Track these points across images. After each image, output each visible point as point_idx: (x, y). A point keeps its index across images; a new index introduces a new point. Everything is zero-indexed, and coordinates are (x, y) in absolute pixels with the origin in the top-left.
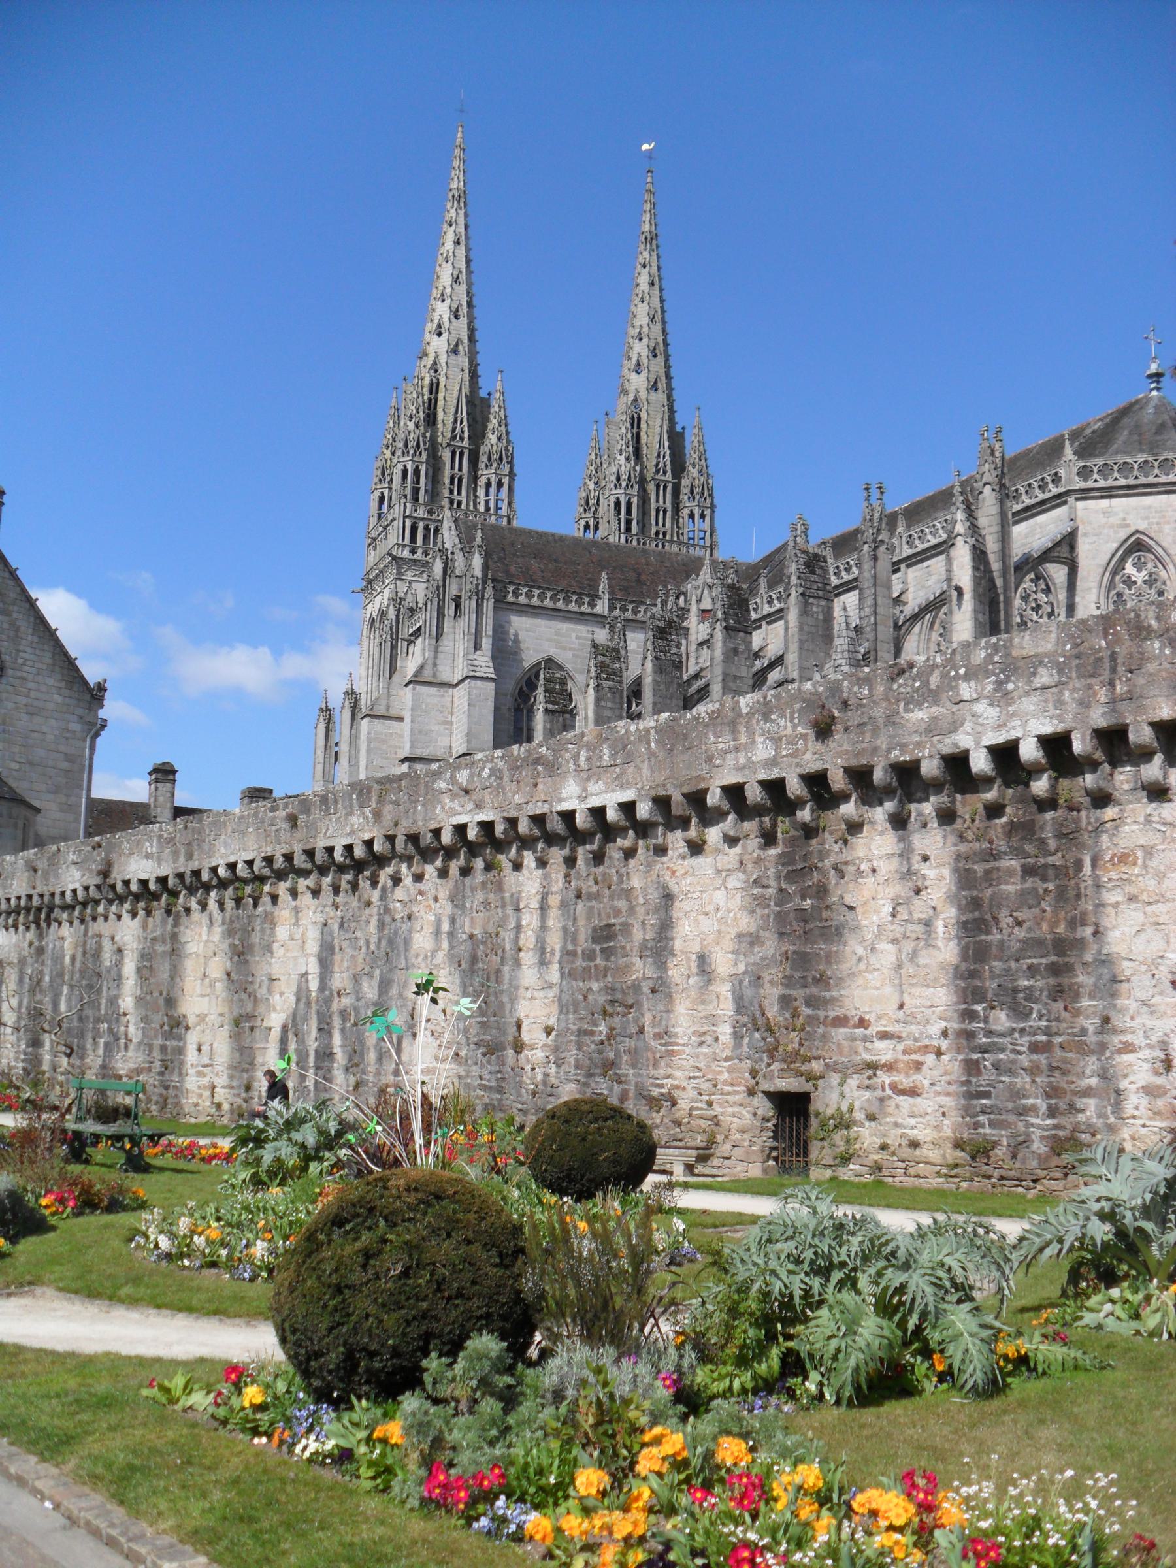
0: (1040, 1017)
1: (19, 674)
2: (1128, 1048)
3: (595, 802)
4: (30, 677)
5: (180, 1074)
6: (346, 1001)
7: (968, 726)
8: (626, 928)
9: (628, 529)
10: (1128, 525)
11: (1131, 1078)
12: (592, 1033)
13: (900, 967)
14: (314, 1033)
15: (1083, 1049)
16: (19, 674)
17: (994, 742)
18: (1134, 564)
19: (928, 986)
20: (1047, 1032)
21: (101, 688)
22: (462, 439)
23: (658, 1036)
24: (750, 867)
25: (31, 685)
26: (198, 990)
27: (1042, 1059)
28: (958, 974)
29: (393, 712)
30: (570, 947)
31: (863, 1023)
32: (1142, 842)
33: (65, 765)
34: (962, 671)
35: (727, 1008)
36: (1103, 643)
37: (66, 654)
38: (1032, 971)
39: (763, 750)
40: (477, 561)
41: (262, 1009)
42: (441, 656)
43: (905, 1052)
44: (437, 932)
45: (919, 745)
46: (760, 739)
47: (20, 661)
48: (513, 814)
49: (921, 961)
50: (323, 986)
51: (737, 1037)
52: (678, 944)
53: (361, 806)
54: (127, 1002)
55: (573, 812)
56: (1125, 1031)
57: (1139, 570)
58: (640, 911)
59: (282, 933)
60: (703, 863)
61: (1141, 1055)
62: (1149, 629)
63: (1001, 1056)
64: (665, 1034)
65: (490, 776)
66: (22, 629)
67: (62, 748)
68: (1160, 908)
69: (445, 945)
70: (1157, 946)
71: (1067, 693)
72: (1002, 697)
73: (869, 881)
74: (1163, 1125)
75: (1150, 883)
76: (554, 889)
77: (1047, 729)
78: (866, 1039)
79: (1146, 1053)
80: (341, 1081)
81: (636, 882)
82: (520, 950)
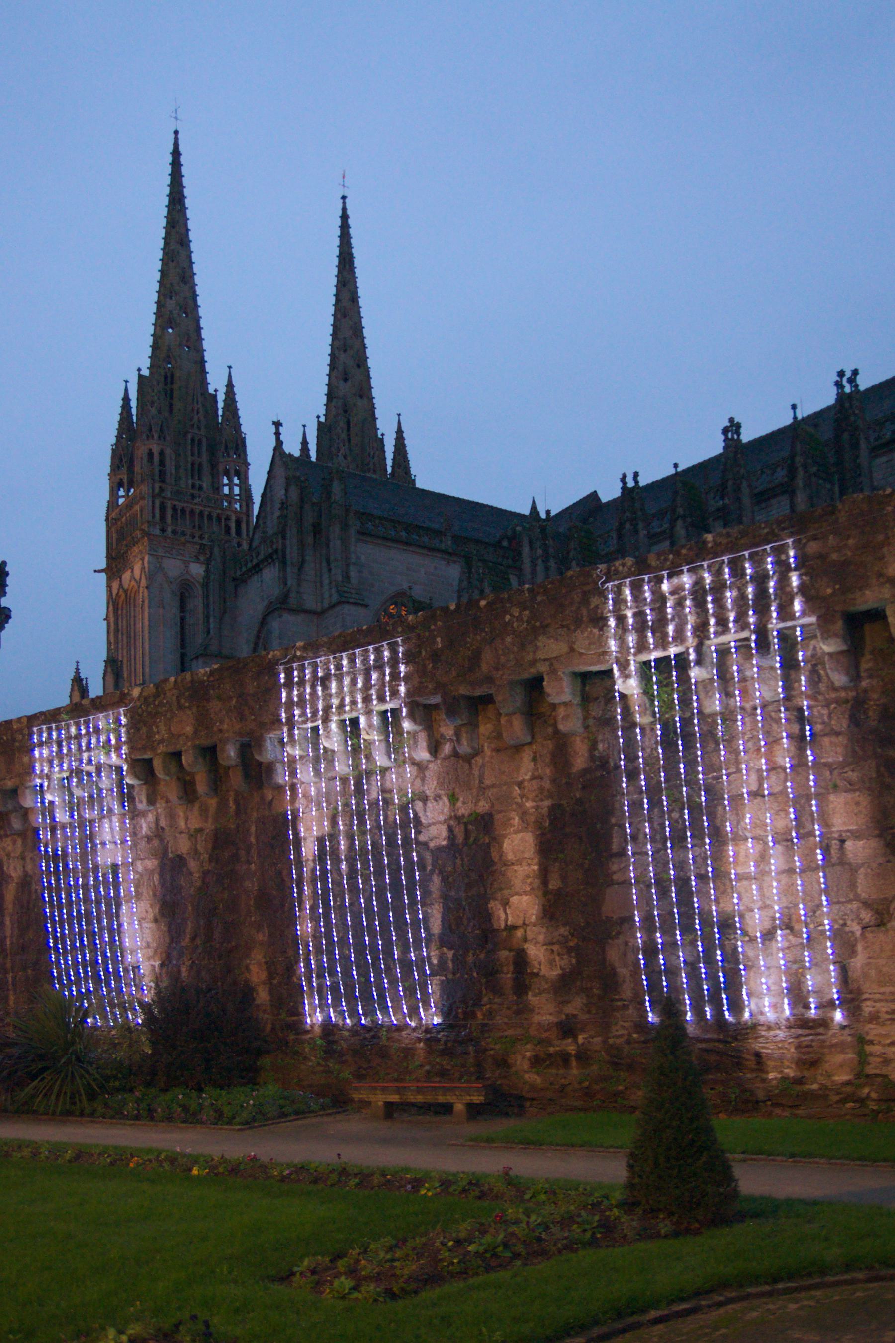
22: (199, 428)
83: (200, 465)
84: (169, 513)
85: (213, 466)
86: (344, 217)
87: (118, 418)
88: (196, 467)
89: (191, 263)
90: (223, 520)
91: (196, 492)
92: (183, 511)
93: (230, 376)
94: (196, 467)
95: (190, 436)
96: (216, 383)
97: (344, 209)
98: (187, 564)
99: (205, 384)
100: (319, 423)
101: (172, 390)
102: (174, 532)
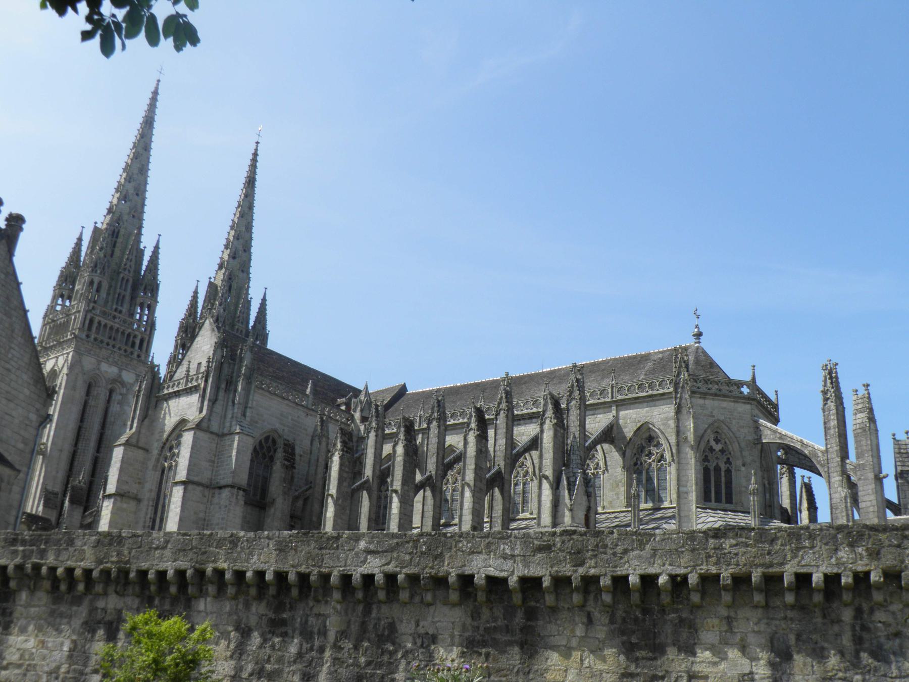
4: (13, 370)
10: (713, 416)
16: (8, 366)
18: (714, 440)
29: (140, 445)
33: (21, 446)
57: (717, 443)
83: (124, 297)
84: (95, 325)
85: (133, 298)
86: (255, 154)
87: (71, 250)
88: (121, 297)
89: (149, 162)
90: (132, 337)
92: (105, 326)
93: (158, 241)
94: (121, 297)
95: (121, 275)
96: (147, 243)
97: (256, 150)
98: (99, 362)
99: (138, 241)
100: (210, 283)
101: (115, 242)
102: (95, 339)
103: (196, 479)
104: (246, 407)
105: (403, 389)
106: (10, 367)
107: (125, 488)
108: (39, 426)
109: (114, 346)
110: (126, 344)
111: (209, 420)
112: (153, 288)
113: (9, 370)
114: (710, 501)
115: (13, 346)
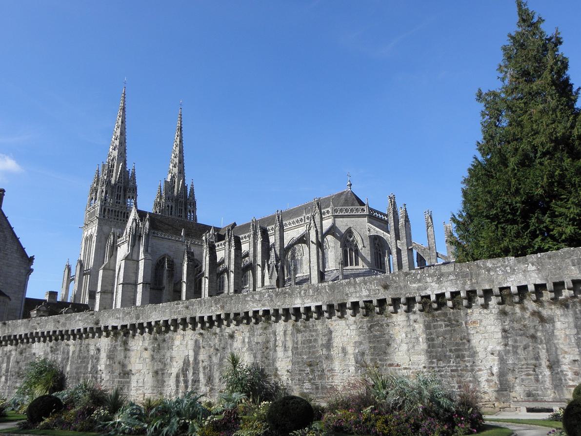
0: (453, 363)
1: (5, 252)
2: (480, 370)
3: (307, 305)
4: (9, 254)
5: (128, 390)
6: (206, 363)
7: (429, 289)
8: (316, 340)
9: (171, 214)
11: (482, 378)
12: (305, 371)
13: (409, 350)
14: (191, 374)
15: (467, 371)
16: (5, 252)
17: (437, 293)
19: (418, 355)
20: (456, 366)
21: (32, 259)
23: (329, 371)
24: (358, 324)
25: (9, 256)
26: (137, 361)
27: (455, 373)
28: (427, 352)
29: (111, 268)
30: (295, 346)
31: (398, 365)
32: (479, 318)
33: (18, 284)
34: (427, 275)
35: (352, 362)
36: (468, 270)
37: (22, 247)
38: (451, 351)
39: (365, 293)
40: (147, 224)
41: (168, 367)
42: (134, 252)
43: (412, 373)
44: (244, 342)
45: (415, 293)
46: (363, 290)
47: (6, 248)
48: (277, 308)
49: (416, 348)
50: (196, 359)
51: (357, 371)
52: (335, 344)
53: (216, 304)
54: (101, 366)
55: (300, 308)
56: (479, 366)
58: (320, 336)
59: (177, 343)
60: (342, 322)
61: (484, 372)
62: (481, 267)
63: (442, 373)
64: (332, 370)
65: (268, 297)
66: (8, 238)
67: (18, 279)
68: (486, 335)
69: (247, 346)
70: (486, 343)
71: (458, 281)
72: (439, 281)
73: (397, 328)
74: (493, 389)
75: (482, 328)
76: (289, 329)
77: (454, 290)
78: (399, 369)
79: (485, 372)
80: (203, 389)
81: (319, 327)
82: (277, 346)
83: (120, 195)
85: (125, 195)
88: (119, 196)
91: (117, 204)
94: (119, 196)
95: (117, 185)
103: (128, 282)
104: (148, 247)
105: (235, 224)
106: (7, 253)
107: (106, 288)
108: (27, 274)
109: (117, 219)
110: (124, 217)
111: (132, 255)
112: (135, 189)
113: (6, 254)
114: (353, 265)
115: (7, 244)
